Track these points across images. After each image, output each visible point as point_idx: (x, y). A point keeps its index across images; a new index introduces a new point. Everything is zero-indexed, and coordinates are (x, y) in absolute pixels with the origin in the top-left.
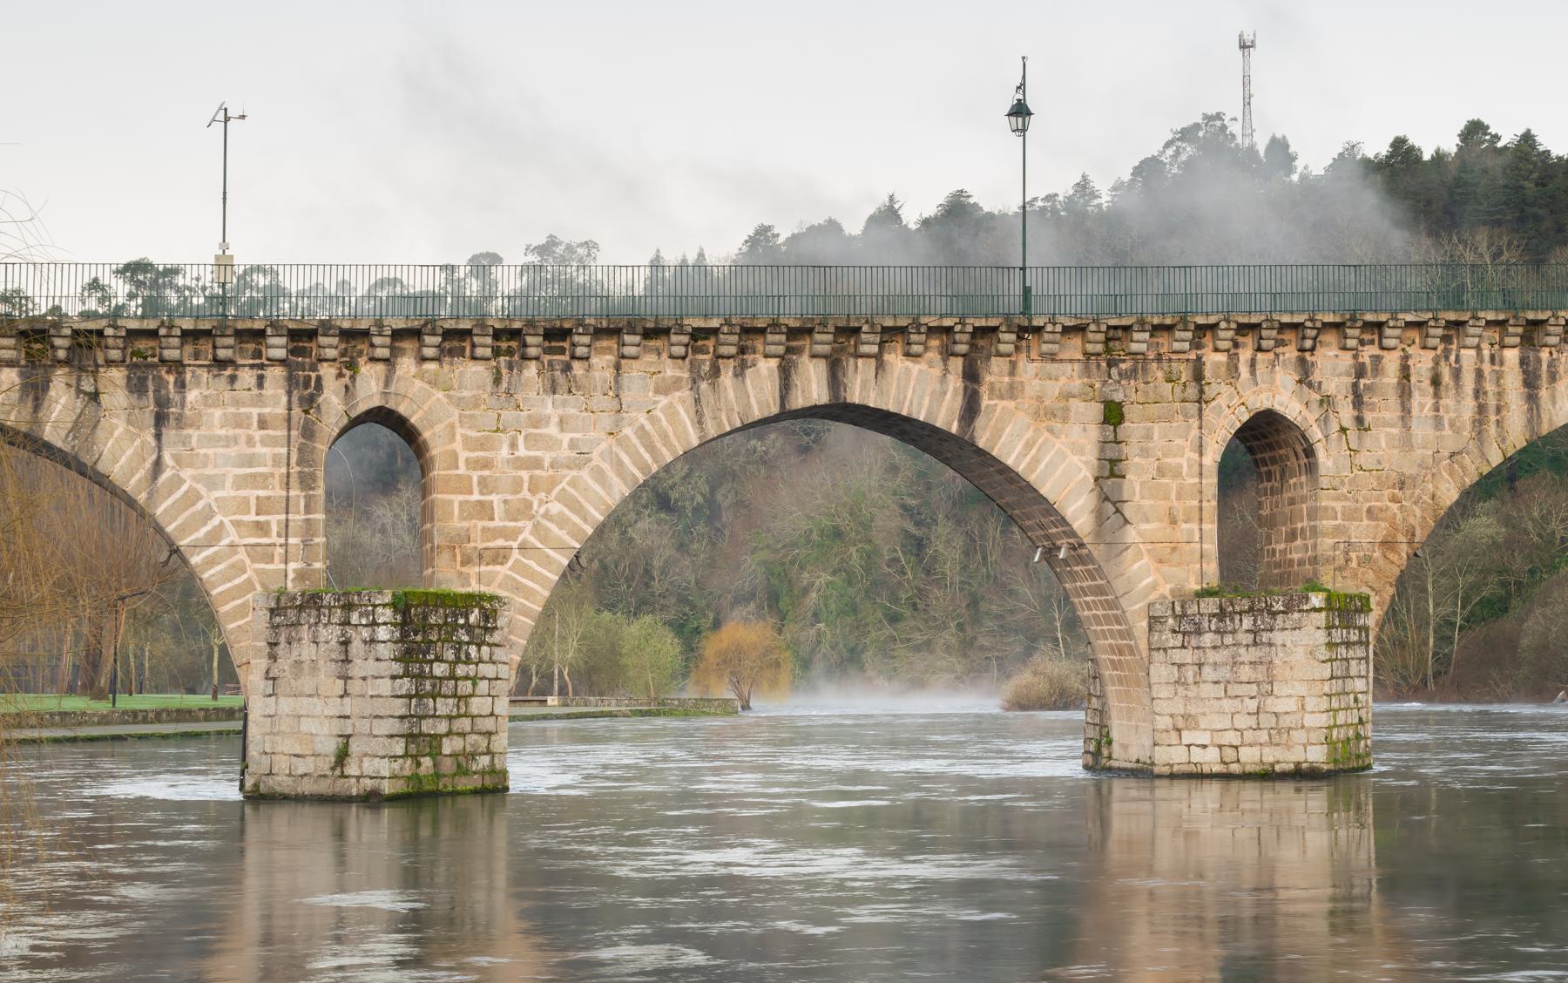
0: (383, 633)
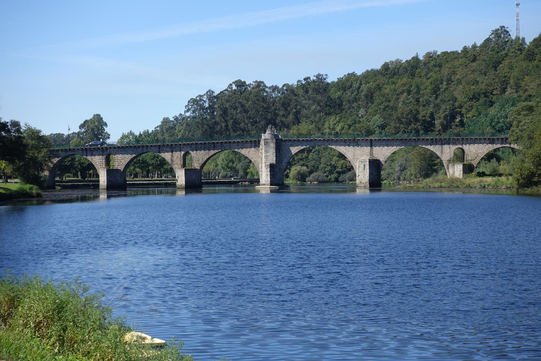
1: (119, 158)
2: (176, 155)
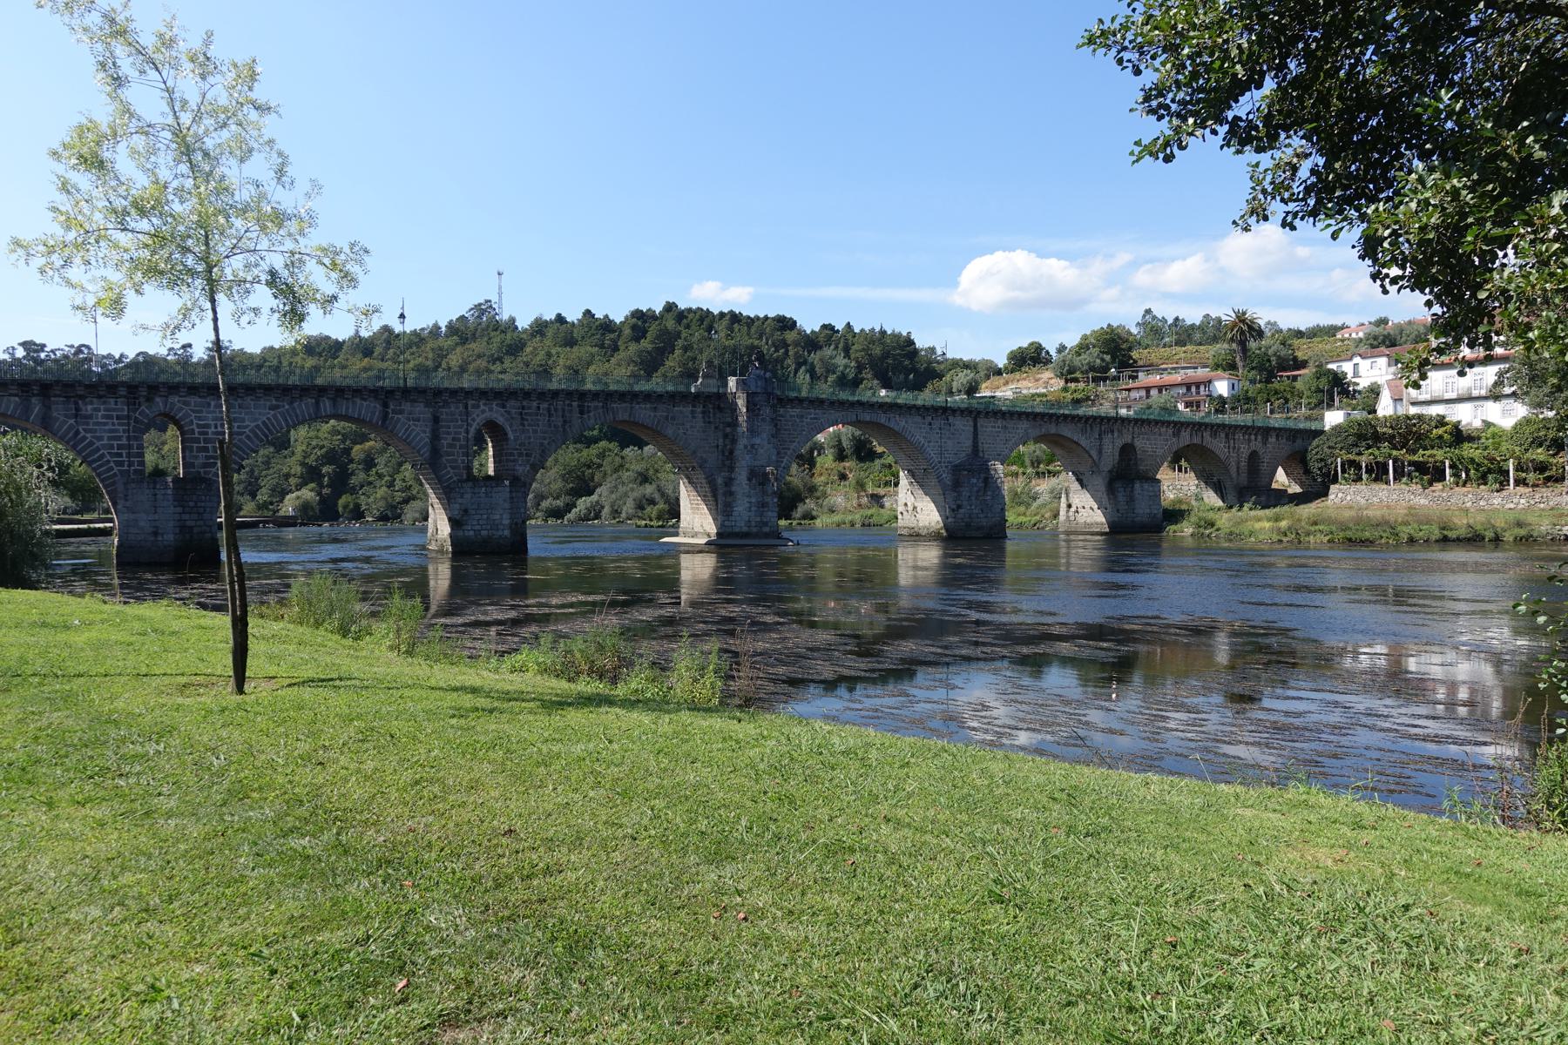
0: (169, 492)
2: (448, 433)
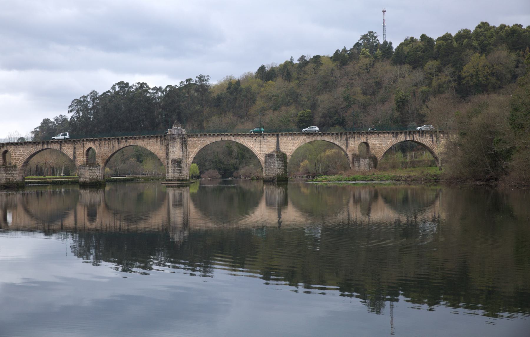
1: (17, 155)
2: (78, 152)
